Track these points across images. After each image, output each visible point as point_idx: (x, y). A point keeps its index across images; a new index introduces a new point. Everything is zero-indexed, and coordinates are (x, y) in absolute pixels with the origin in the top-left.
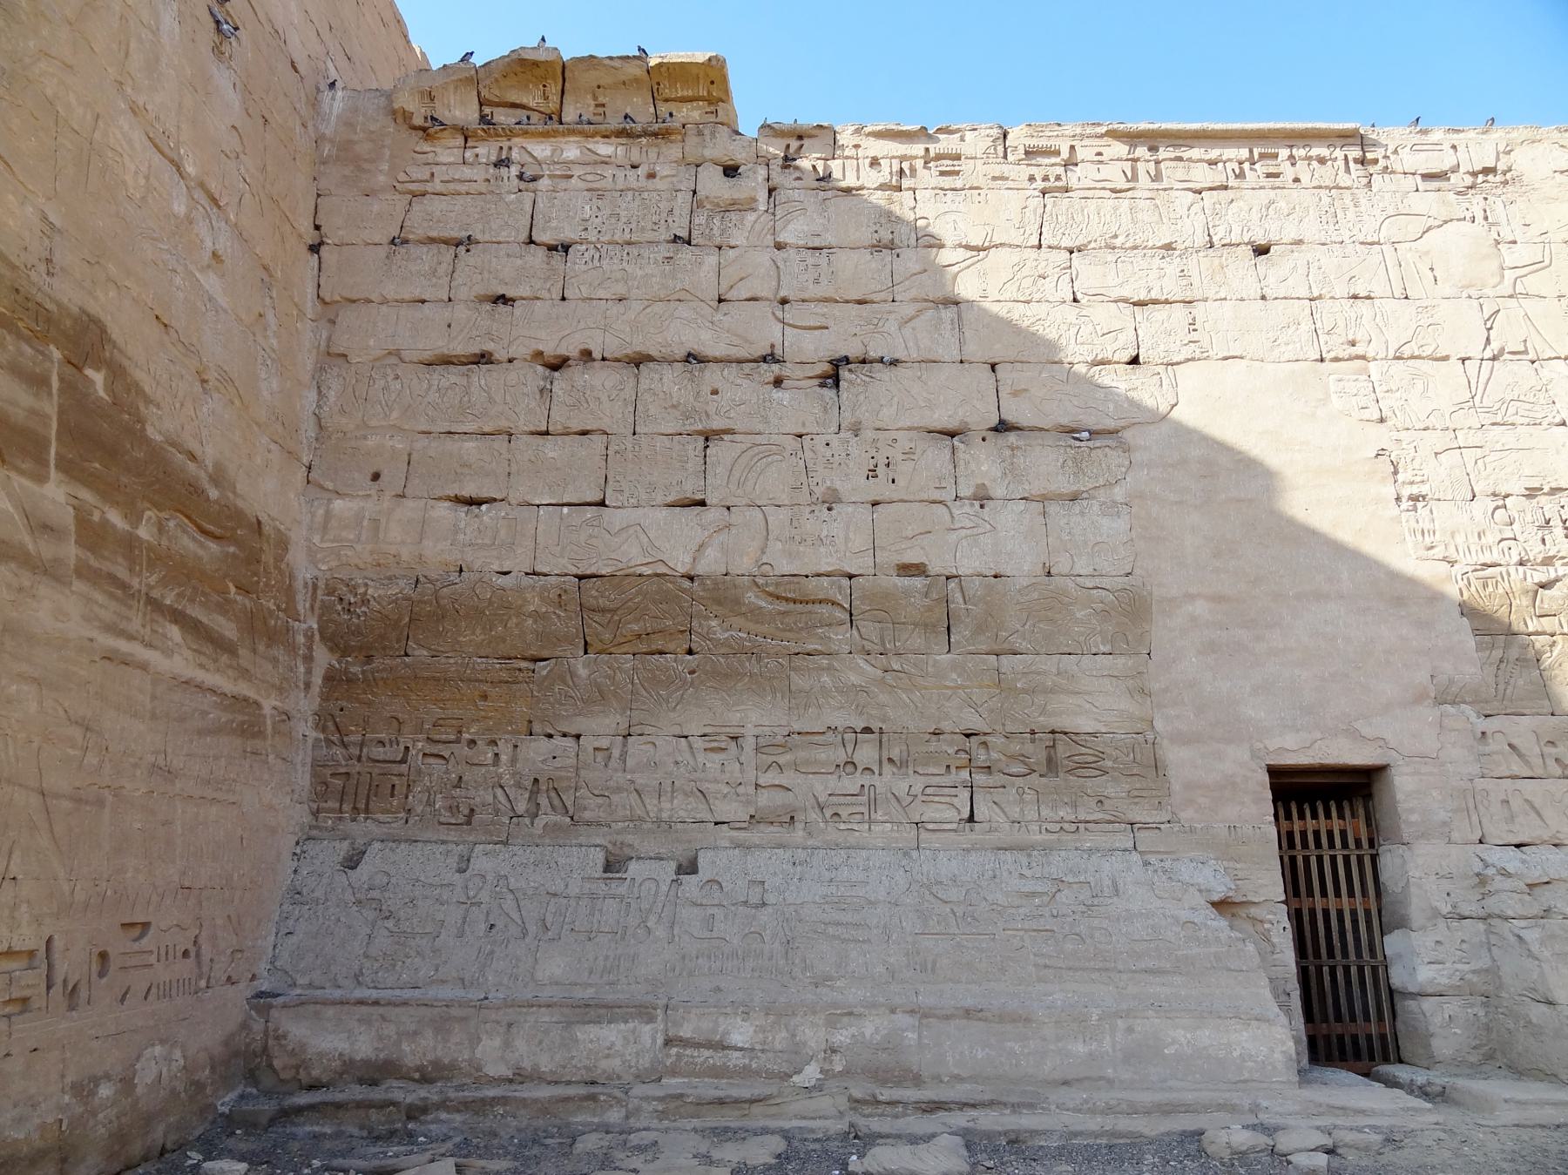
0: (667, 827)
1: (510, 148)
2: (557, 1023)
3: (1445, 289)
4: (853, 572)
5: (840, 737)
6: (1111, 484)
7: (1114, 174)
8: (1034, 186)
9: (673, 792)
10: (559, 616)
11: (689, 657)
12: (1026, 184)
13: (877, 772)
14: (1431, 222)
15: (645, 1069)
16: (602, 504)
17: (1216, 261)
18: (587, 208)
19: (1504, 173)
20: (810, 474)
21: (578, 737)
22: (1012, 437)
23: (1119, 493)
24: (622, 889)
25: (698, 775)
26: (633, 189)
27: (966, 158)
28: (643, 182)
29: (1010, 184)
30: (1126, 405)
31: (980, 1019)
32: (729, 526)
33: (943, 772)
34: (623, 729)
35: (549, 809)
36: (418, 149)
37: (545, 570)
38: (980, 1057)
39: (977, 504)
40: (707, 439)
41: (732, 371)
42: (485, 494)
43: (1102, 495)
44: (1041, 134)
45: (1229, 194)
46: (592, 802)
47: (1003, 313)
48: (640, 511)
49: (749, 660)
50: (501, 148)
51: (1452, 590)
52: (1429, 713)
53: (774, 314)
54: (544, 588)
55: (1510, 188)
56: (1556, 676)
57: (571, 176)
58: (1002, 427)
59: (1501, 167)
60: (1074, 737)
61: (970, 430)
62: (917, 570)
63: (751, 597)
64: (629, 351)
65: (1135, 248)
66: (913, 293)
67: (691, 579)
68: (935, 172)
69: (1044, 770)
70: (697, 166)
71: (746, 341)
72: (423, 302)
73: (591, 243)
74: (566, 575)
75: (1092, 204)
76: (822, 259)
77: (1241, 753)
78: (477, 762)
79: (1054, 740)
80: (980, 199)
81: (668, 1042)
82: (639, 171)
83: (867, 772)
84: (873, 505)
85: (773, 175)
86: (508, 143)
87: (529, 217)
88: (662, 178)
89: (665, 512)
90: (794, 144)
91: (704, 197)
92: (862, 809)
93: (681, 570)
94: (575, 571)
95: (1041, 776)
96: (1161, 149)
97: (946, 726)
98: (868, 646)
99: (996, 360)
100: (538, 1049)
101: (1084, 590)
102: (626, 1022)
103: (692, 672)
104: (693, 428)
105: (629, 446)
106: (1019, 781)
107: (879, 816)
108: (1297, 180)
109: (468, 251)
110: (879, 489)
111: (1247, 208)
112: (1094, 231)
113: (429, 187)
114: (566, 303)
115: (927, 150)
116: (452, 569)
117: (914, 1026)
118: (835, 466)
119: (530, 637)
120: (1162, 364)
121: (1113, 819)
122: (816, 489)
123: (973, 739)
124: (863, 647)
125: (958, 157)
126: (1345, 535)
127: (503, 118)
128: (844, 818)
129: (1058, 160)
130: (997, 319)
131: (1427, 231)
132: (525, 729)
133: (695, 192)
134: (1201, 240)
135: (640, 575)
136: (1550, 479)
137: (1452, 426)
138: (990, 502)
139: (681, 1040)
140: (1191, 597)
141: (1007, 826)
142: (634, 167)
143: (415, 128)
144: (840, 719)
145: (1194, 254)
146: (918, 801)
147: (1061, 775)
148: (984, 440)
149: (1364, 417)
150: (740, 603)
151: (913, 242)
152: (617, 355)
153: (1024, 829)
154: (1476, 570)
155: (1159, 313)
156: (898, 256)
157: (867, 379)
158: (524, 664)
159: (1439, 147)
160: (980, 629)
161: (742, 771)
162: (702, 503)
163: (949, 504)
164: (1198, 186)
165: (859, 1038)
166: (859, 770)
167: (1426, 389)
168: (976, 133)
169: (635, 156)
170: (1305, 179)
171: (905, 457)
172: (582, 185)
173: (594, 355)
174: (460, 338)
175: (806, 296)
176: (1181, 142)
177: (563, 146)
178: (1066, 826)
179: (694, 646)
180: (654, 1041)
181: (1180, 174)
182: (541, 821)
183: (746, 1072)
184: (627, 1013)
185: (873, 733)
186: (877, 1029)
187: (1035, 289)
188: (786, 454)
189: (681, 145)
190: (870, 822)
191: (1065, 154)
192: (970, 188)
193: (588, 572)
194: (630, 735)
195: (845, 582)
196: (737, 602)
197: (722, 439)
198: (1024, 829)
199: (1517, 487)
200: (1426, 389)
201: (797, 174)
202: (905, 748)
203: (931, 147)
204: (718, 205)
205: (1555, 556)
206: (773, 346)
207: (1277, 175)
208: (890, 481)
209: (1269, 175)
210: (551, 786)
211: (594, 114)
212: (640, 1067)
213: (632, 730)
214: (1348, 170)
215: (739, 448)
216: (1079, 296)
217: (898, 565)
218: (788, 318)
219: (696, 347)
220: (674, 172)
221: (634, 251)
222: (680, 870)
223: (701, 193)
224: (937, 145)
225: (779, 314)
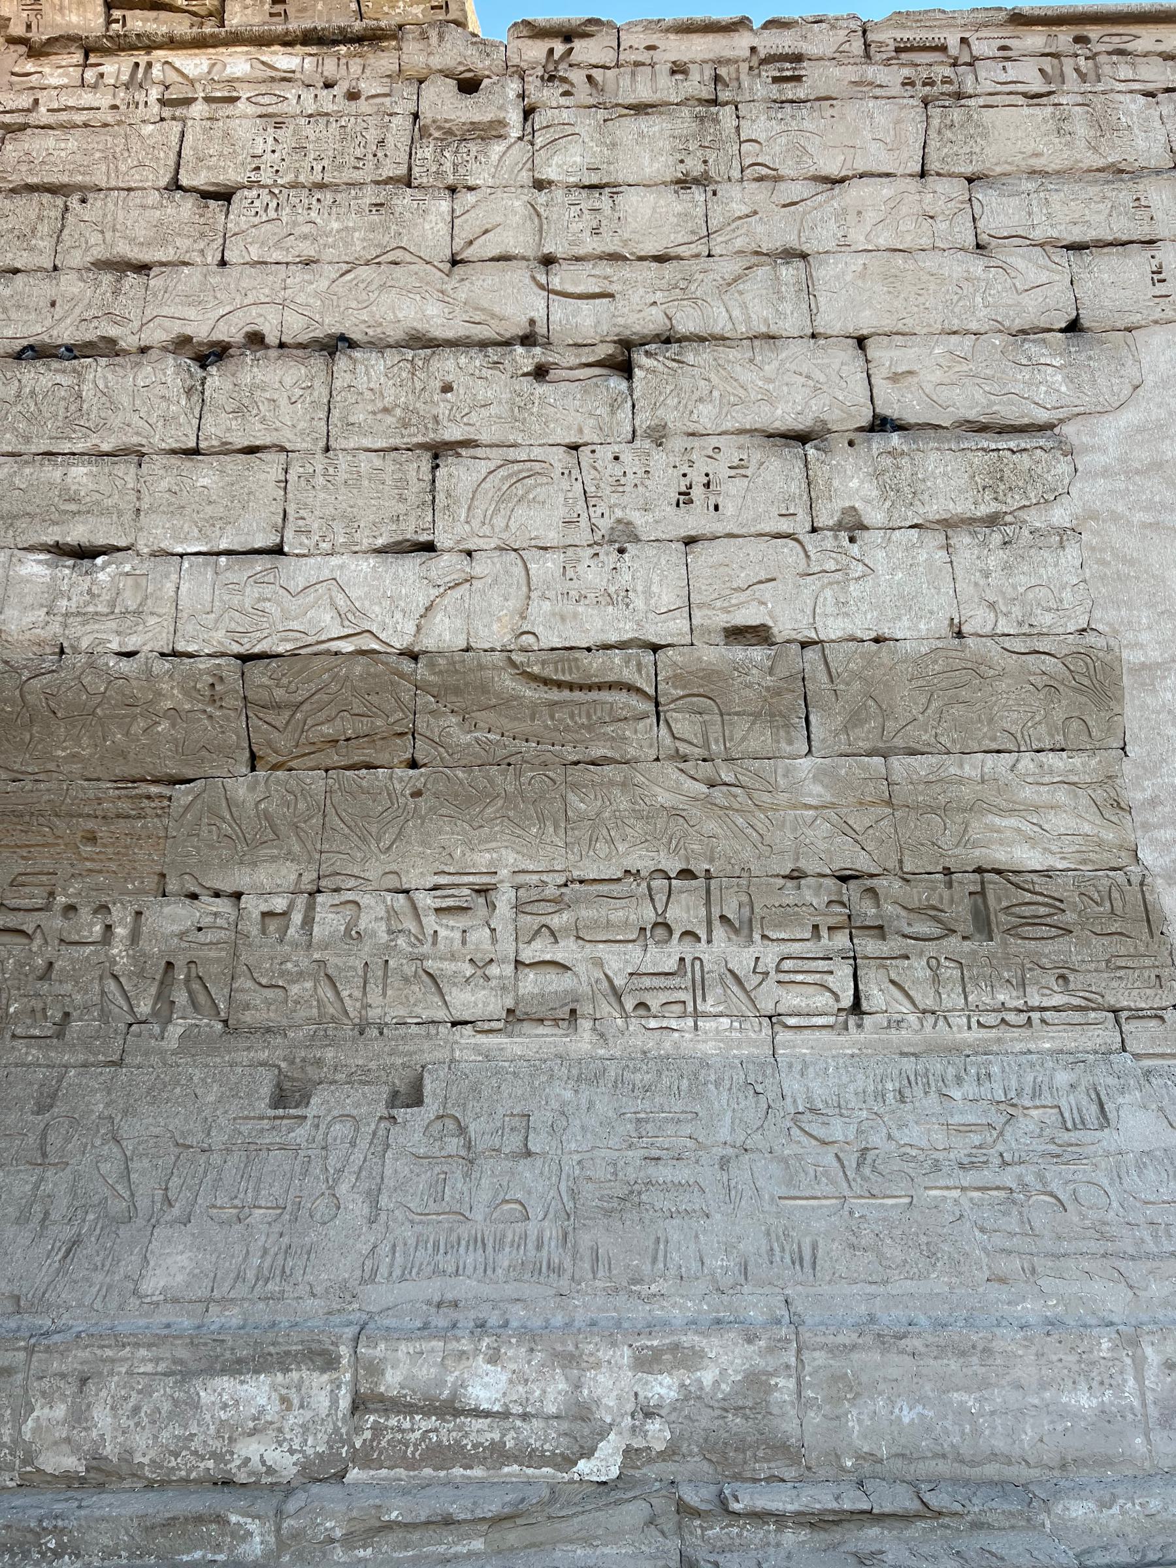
0: (375, 1032)
1: (149, 65)
2: (165, 1374)
4: (655, 640)
5: (644, 885)
6: (1046, 501)
9: (386, 976)
10: (210, 717)
11: (411, 772)
13: (704, 937)
15: (320, 1456)
16: (278, 550)
18: (260, 140)
20: (592, 502)
21: (238, 896)
22: (895, 439)
23: (1060, 515)
24: (301, 1133)
25: (426, 948)
26: (327, 114)
28: (342, 104)
29: (878, 92)
31: (902, 1352)
32: (469, 580)
33: (808, 935)
34: (307, 883)
35: (190, 1010)
36: (16, 69)
37: (190, 649)
38: (906, 1420)
39: (844, 535)
40: (436, 457)
41: (473, 361)
42: (101, 540)
46: (257, 997)
48: (335, 561)
49: (504, 773)
50: (137, 65)
53: (534, 278)
54: (192, 676)
57: (238, 98)
58: (881, 424)
60: (1012, 878)
61: (829, 431)
62: (757, 634)
63: (508, 682)
64: (319, 334)
66: (739, 243)
67: (415, 657)
69: (967, 927)
70: (421, 82)
71: (493, 316)
72: (16, 271)
73: (264, 187)
74: (223, 655)
76: (604, 202)
78: (76, 938)
79: (982, 883)
81: (359, 1405)
82: (335, 90)
83: (688, 939)
84: (686, 544)
85: (531, 89)
86: (146, 58)
87: (173, 157)
88: (368, 98)
89: (373, 560)
90: (560, 48)
91: (429, 121)
92: (682, 995)
93: (399, 643)
94: (236, 649)
95: (964, 938)
97: (810, 865)
98: (684, 748)
99: (865, 332)
100: (131, 1423)
101: (1014, 656)
102: (286, 1370)
103: (417, 794)
104: (415, 440)
105: (319, 468)
106: (931, 948)
107: (708, 1007)
109: (83, 201)
110: (695, 521)
113: (32, 119)
114: (227, 270)
116: (48, 650)
117: (788, 1367)
118: (627, 489)
119: (166, 749)
121: (1083, 1003)
122: (600, 523)
123: (853, 884)
124: (677, 750)
125: (798, 58)
127: (140, 23)
128: (653, 1010)
132: (153, 886)
133: (416, 116)
135: (336, 654)
138: (866, 534)
139: (382, 1398)
141: (912, 1018)
142: (328, 85)
143: (13, 41)
144: (642, 860)
146: (771, 981)
147: (998, 937)
148: (851, 444)
150: (488, 692)
151: (736, 174)
152: (304, 338)
153: (941, 1022)
156: (715, 193)
157: (675, 365)
158: (154, 789)
160: (855, 719)
161: (494, 941)
162: (429, 547)
163: (801, 537)
165: (692, 1389)
166: (676, 935)
169: (330, 68)
171: (733, 472)
172: (251, 110)
173: (267, 340)
174: (68, 321)
175: (581, 251)
177: (228, 60)
178: (1011, 1017)
179: (420, 757)
180: (334, 1402)
182: (175, 1030)
183: (497, 1454)
184: (287, 1353)
185: (695, 877)
186: (723, 1372)
188: (556, 474)
189: (396, 53)
190: (696, 1015)
193: (256, 650)
194: (319, 891)
195: (648, 657)
196: (484, 689)
197: (459, 455)
198: (941, 1022)
201: (566, 87)
202: (745, 899)
204: (450, 132)
206: (532, 322)
208: (712, 508)
210: (193, 974)
211: (271, 15)
212: (310, 1451)
213: (323, 883)
215: (483, 467)
217: (726, 630)
218: (556, 283)
219: (419, 327)
220: (386, 90)
221: (328, 197)
222: (395, 1101)
223: (427, 116)
225: (542, 279)
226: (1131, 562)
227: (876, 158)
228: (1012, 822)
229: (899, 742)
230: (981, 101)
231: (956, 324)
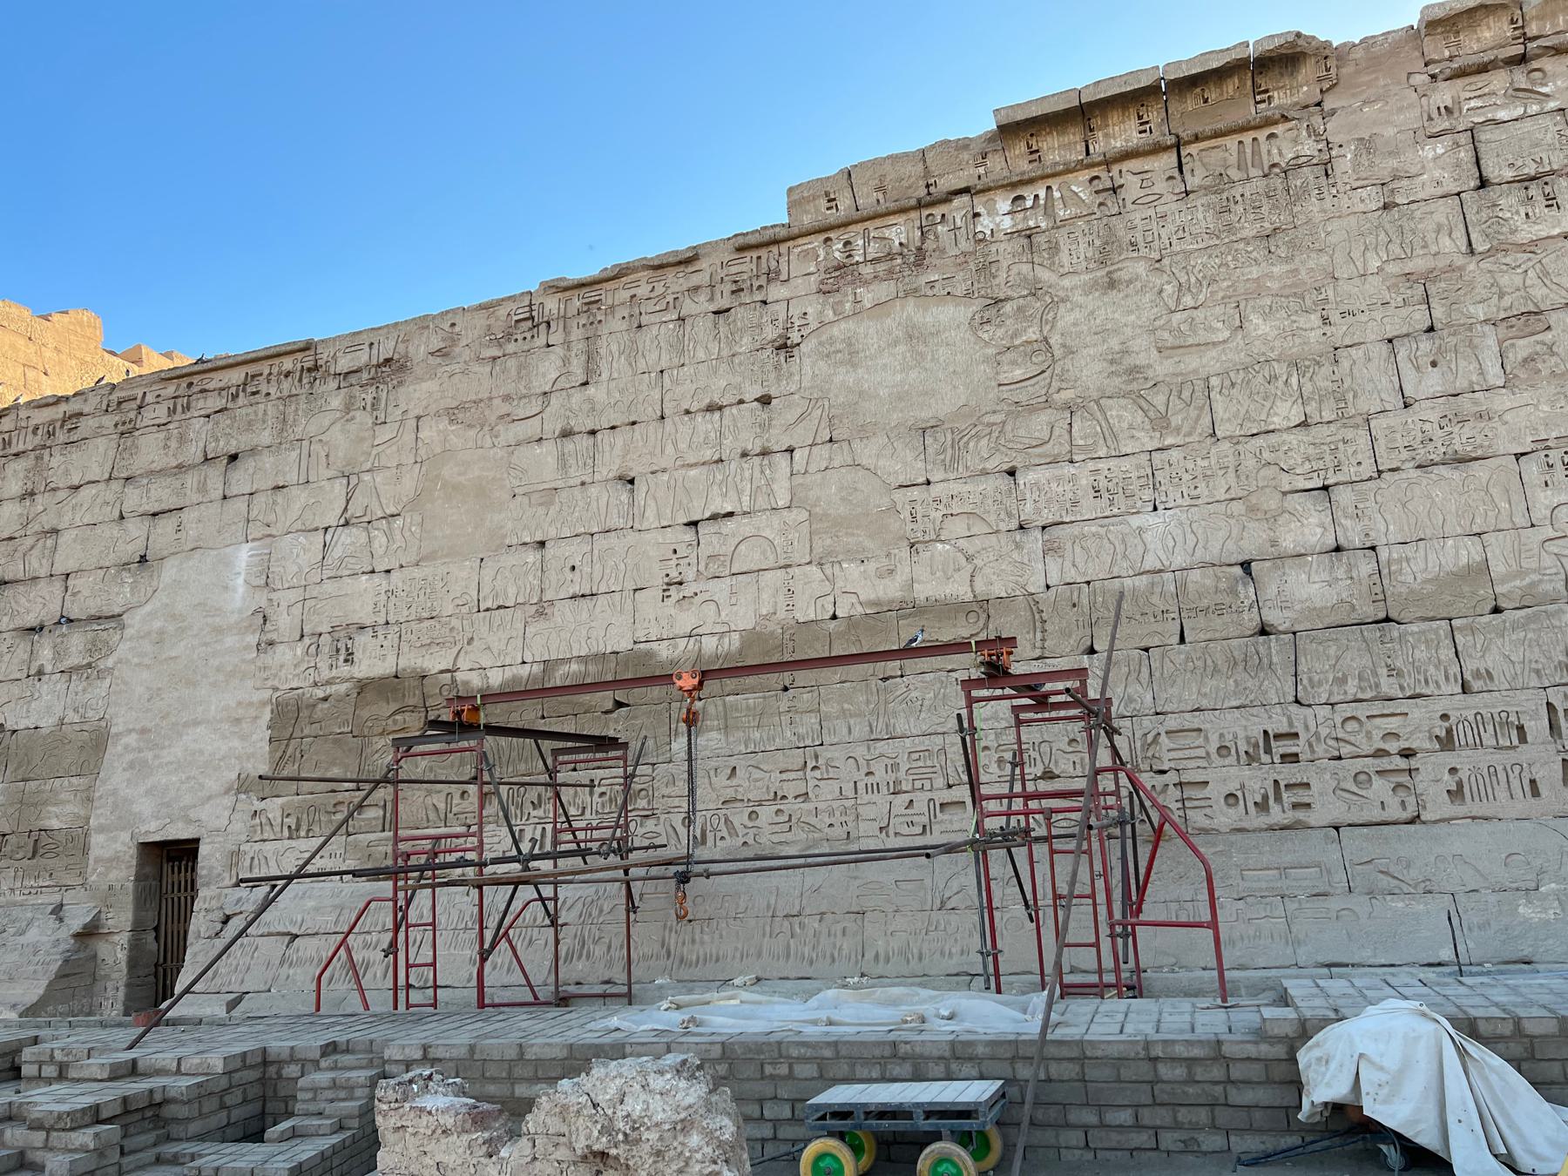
7: (161, 412)
23: (110, 662)
52: (228, 801)
77: (125, 836)
125: (81, 414)
164: (209, 411)
170: (272, 391)
199: (325, 628)
226: (126, 683)
227: (96, 472)
228: (54, 809)
229: (32, 775)
230: (140, 432)
231: (102, 563)
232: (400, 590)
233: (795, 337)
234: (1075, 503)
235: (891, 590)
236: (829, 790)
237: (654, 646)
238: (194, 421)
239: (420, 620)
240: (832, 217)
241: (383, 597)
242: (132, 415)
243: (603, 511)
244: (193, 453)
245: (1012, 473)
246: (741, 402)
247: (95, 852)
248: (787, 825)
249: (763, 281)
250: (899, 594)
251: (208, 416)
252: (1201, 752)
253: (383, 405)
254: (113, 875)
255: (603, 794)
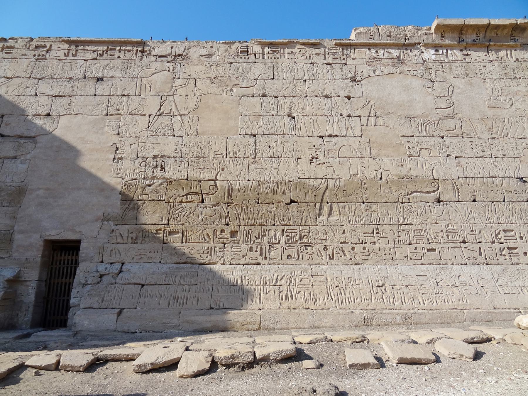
3: (152, 93)
7: (61, 54)
8: (34, 58)
12: (32, 57)
14: (156, 71)
17: (84, 83)
19: (185, 56)
23: (28, 157)
27: (16, 48)
29: (27, 57)
30: (40, 129)
43: (23, 158)
44: (42, 41)
45: (96, 61)
47: (11, 99)
51: (119, 187)
55: (185, 61)
56: (141, 213)
59: (184, 54)
65: (60, 78)
68: (4, 53)
75: (51, 64)
80: (15, 62)
96: (79, 46)
99: (4, 114)
108: (119, 57)
111: (99, 66)
112: (48, 72)
115: (4, 45)
120: (56, 116)
126: (94, 171)
129: (45, 49)
130: (8, 101)
131: (154, 74)
134: (81, 76)
136: (162, 153)
137: (138, 136)
140: (39, 189)
145: (78, 81)
149: (113, 133)
154: (129, 181)
155: (60, 100)
159: (167, 47)
167: (135, 125)
168: (22, 40)
170: (122, 56)
176: (86, 44)
181: (82, 55)
187: (24, 91)
191: (48, 48)
192: (14, 58)
199: (150, 155)
200: (135, 125)
203: (5, 44)
205: (155, 177)
207: (113, 55)
209: (111, 55)
214: (136, 54)
216: (37, 94)
224: (8, 44)
232: (188, 145)
233: (358, 78)
234: (466, 151)
235: (403, 171)
236: (383, 241)
237: (308, 180)
238: (79, 61)
239: (198, 158)
240: (371, 41)
241: (180, 146)
242: (44, 53)
243: (282, 126)
244: (79, 73)
245: (443, 138)
246: (339, 96)
247: (15, 244)
248: (368, 253)
249: (345, 57)
250: (406, 173)
251: (86, 61)
252: (514, 238)
253: (179, 71)
254: (28, 254)
255: (288, 236)
